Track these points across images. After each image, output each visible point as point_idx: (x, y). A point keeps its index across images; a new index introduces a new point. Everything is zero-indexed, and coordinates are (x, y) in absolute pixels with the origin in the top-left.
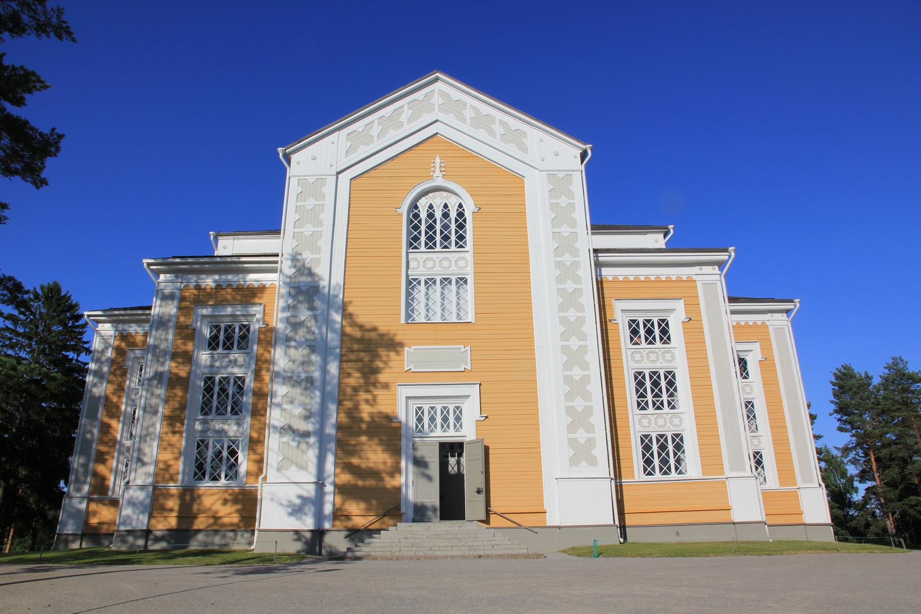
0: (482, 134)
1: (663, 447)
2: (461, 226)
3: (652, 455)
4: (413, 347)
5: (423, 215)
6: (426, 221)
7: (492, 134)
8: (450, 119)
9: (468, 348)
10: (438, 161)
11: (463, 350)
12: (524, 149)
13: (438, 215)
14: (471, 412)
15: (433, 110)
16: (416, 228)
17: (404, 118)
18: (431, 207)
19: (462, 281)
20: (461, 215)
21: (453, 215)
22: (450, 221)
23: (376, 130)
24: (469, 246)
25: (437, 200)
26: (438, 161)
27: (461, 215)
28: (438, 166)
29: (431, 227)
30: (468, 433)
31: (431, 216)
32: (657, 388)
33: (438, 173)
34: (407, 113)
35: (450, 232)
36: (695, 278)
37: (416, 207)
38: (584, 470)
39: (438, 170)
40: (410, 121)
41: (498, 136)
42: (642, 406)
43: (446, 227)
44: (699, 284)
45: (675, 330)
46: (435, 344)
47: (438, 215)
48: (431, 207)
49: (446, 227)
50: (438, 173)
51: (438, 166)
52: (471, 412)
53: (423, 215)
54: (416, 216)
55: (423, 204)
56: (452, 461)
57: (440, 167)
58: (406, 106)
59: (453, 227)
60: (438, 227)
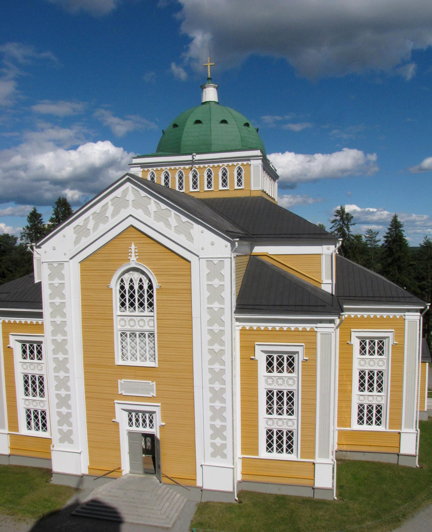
1: (280, 438)
2: (151, 296)
3: (272, 441)
4: (123, 380)
5: (127, 287)
6: (129, 292)
7: (168, 225)
9: (154, 383)
10: (133, 247)
11: (151, 384)
12: (190, 238)
13: (136, 287)
17: (109, 213)
18: (131, 281)
19: (152, 334)
20: (151, 287)
21: (146, 287)
22: (144, 292)
23: (91, 225)
25: (136, 276)
26: (133, 247)
27: (151, 287)
28: (133, 251)
29: (132, 296)
30: (155, 431)
31: (131, 288)
32: (280, 401)
33: (133, 258)
34: (111, 209)
35: (144, 300)
36: (316, 329)
37: (122, 281)
38: (218, 462)
39: (133, 255)
41: (173, 228)
42: (269, 410)
43: (141, 296)
44: (319, 335)
45: (298, 364)
46: (136, 379)
47: (136, 287)
48: (131, 281)
49: (141, 296)
50: (133, 258)
51: (133, 251)
52: (158, 420)
53: (127, 287)
54: (122, 288)
55: (126, 277)
56: (149, 444)
57: (135, 252)
58: (110, 203)
59: (146, 296)
60: (136, 296)
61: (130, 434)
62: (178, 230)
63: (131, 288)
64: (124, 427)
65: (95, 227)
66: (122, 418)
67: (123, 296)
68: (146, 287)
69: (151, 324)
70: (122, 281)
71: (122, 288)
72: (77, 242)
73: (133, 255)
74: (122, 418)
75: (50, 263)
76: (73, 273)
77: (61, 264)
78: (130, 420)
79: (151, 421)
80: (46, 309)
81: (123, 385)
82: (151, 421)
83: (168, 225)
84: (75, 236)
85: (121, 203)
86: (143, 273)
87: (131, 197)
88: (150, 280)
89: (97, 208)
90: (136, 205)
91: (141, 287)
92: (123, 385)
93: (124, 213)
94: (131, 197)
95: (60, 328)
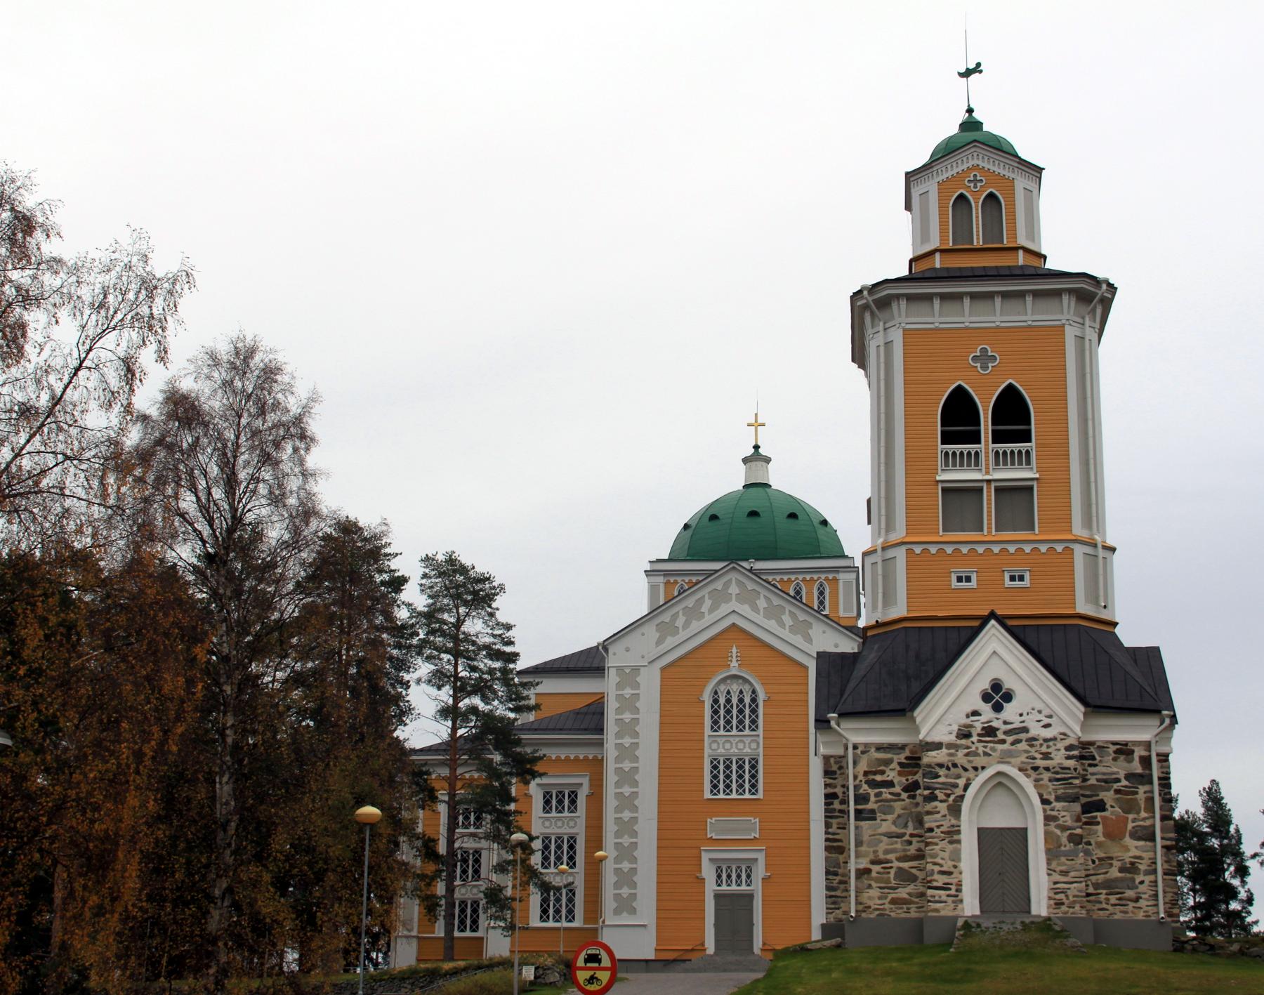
0: (772, 625)
2: (754, 711)
5: (722, 701)
8: (745, 609)
10: (734, 650)
12: (809, 640)
13: (735, 700)
14: (760, 871)
15: (731, 600)
16: (716, 712)
17: (705, 609)
18: (728, 692)
21: (747, 700)
24: (760, 731)
25: (735, 687)
26: (734, 650)
27: (754, 700)
29: (728, 712)
31: (728, 701)
33: (734, 664)
37: (716, 693)
39: (734, 659)
40: (711, 611)
47: (735, 700)
48: (728, 692)
50: (734, 664)
52: (760, 871)
53: (722, 701)
54: (716, 701)
55: (723, 689)
61: (718, 897)
62: (793, 630)
63: (728, 701)
64: (711, 887)
65: (687, 625)
66: (708, 872)
67: (716, 712)
68: (747, 700)
69: (754, 745)
70: (716, 693)
71: (716, 701)
72: (659, 643)
73: (734, 659)
74: (708, 872)
75: (620, 669)
76: (650, 685)
77: (636, 670)
78: (719, 876)
79: (749, 876)
80: (611, 727)
81: (714, 826)
82: (749, 876)
83: (782, 625)
84: (658, 635)
85: (720, 598)
86: (746, 681)
87: (734, 590)
88: (754, 692)
89: (690, 602)
90: (740, 599)
91: (741, 701)
92: (714, 826)
93: (724, 609)
94: (734, 590)
95: (628, 753)
